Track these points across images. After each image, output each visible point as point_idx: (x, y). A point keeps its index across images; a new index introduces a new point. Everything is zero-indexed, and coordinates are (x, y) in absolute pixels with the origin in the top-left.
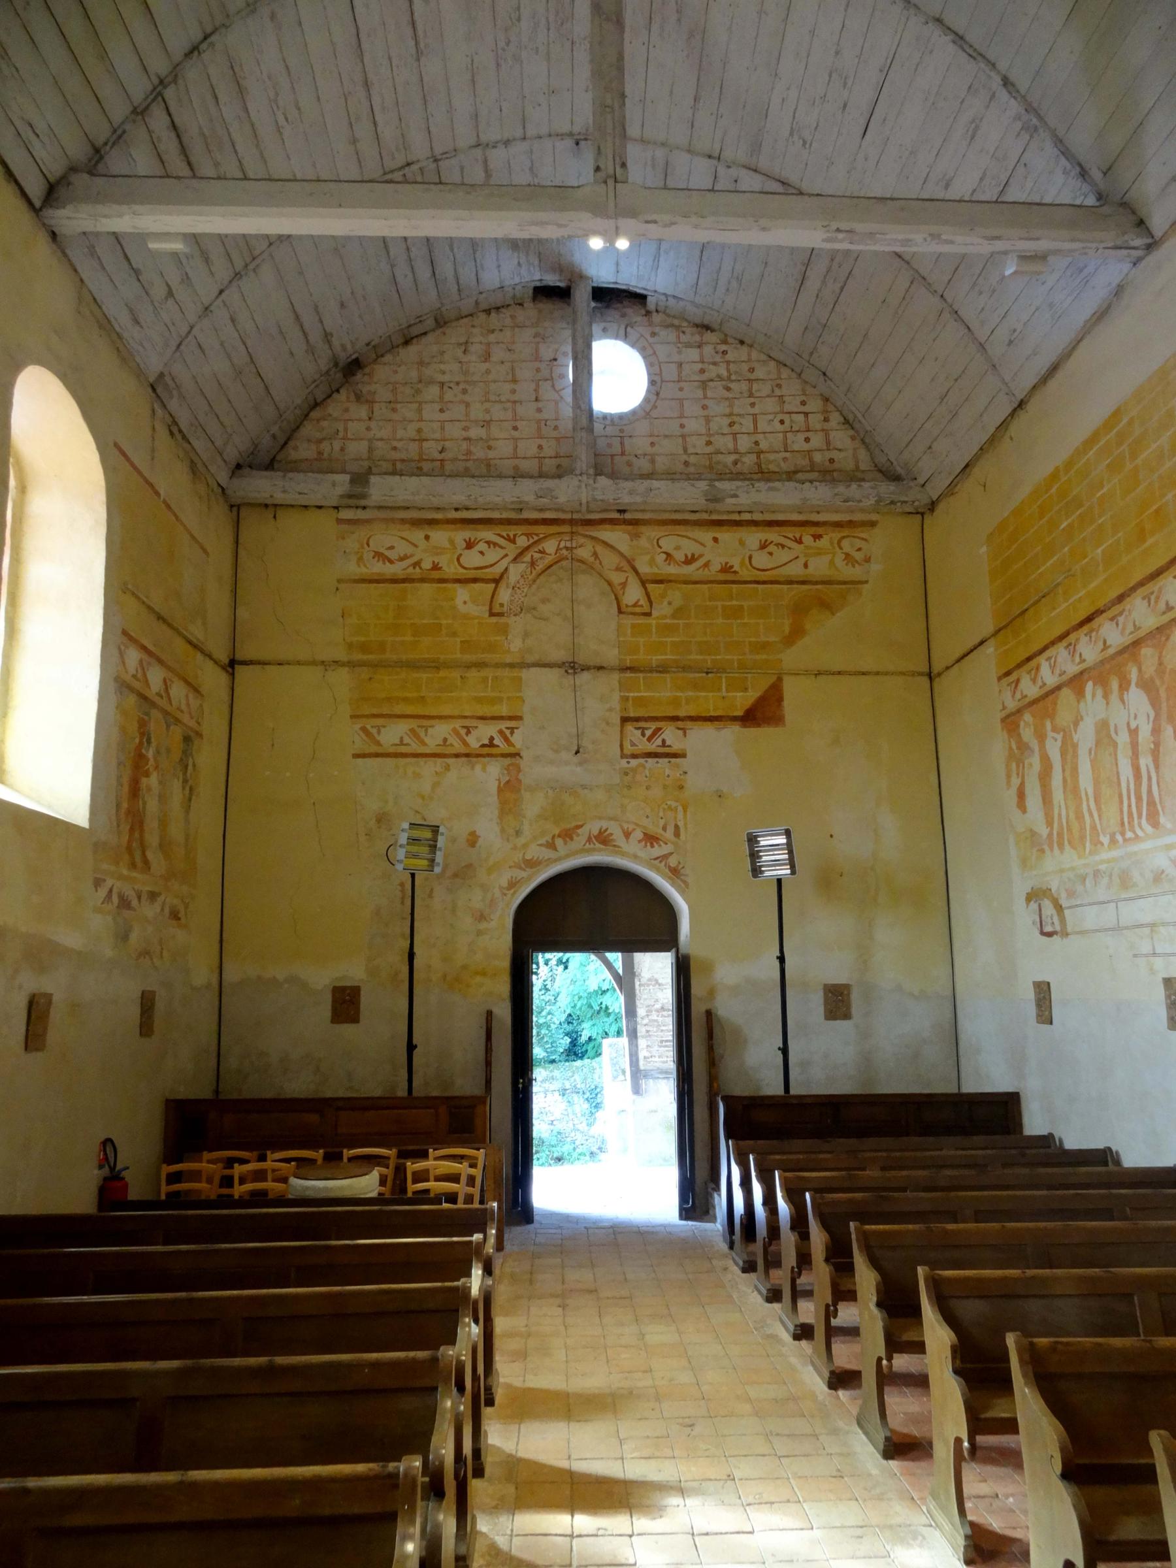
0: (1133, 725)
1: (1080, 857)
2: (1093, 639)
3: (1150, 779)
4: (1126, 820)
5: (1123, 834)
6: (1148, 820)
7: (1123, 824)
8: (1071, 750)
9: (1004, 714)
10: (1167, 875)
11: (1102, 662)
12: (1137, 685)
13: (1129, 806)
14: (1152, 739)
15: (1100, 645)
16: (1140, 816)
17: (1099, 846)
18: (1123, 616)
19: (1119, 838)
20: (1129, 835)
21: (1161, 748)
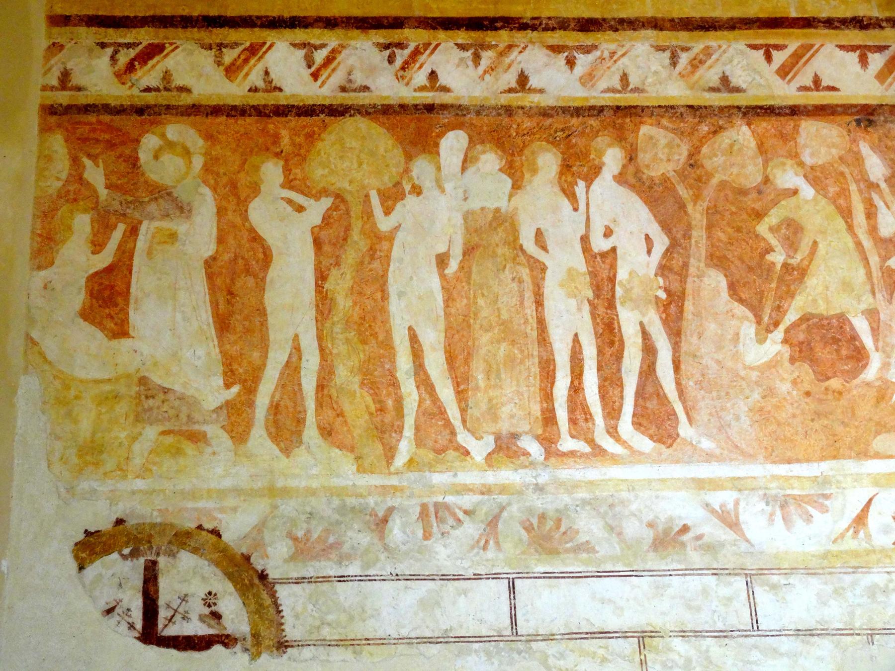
0: (600, 244)
1: (361, 470)
2: (485, 63)
3: (649, 350)
4: (562, 415)
5: (548, 442)
6: (637, 424)
7: (549, 418)
8: (358, 241)
9: (63, 98)
10: (699, 537)
11: (509, 110)
12: (620, 179)
13: (576, 388)
14: (661, 280)
15: (510, 79)
16: (612, 412)
17: (451, 454)
18: (591, 57)
19: (535, 449)
20: (567, 444)
21: (689, 306)
